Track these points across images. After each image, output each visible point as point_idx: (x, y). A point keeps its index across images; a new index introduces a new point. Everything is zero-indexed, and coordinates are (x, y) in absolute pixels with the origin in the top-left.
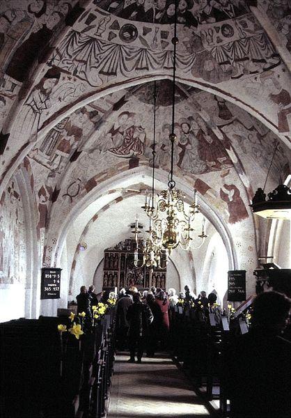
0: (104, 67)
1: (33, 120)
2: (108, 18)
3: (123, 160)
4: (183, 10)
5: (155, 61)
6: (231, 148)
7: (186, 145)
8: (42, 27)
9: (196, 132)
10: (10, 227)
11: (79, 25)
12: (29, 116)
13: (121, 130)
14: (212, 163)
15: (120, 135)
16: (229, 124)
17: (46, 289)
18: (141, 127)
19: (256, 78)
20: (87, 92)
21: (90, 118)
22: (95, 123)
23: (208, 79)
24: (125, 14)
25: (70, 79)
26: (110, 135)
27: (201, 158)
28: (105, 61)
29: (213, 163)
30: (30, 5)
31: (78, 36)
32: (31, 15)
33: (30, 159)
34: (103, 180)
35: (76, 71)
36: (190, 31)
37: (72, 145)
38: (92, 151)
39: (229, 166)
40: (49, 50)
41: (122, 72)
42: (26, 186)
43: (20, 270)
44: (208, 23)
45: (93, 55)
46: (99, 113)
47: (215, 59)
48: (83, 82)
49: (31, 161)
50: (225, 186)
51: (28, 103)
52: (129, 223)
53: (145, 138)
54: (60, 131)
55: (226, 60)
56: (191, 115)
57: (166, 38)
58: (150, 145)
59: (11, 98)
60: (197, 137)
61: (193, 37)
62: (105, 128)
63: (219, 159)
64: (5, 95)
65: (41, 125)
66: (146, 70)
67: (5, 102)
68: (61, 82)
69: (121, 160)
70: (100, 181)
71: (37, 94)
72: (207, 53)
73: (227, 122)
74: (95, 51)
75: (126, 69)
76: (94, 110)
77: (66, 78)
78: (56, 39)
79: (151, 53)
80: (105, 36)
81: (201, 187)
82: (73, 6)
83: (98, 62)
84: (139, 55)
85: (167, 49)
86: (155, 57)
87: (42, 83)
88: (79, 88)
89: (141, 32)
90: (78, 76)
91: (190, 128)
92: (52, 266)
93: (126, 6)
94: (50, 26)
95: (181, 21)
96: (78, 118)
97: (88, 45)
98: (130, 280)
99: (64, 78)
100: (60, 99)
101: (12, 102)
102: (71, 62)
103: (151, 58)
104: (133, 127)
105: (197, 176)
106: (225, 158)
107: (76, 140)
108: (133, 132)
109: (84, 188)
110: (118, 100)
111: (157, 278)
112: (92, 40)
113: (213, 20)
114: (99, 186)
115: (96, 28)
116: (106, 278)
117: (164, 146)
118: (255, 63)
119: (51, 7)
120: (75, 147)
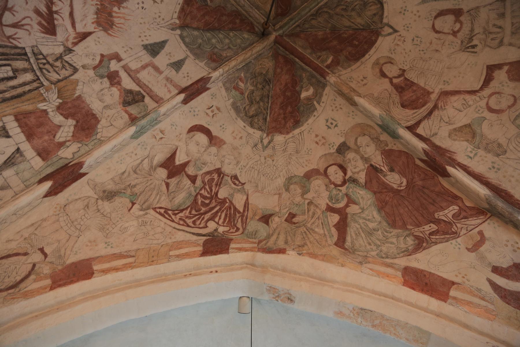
7: (347, 206)
9: (362, 177)
13: (191, 170)
14: (427, 227)
15: (187, 182)
16: (430, 113)
18: (235, 177)
21: (126, 103)
22: (133, 120)
26: (163, 173)
27: (393, 225)
37: (61, 145)
39: (473, 222)
46: (147, 99)
50: (496, 270)
53: (246, 205)
54: (46, 83)
56: (342, 140)
58: (257, 218)
60: (367, 186)
63: (440, 215)
70: (105, 272)
73: (423, 111)
91: (345, 173)
104: (219, 171)
106: (454, 209)
107: (76, 137)
108: (219, 185)
109: (46, 277)
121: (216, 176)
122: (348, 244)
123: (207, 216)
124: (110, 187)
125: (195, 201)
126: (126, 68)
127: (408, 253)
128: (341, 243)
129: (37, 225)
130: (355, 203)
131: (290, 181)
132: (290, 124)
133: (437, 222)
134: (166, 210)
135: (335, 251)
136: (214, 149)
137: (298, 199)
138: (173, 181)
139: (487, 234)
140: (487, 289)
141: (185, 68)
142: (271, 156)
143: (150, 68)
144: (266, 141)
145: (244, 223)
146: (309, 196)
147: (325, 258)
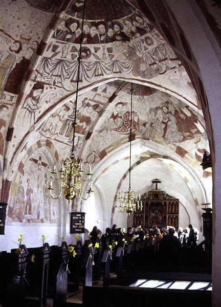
0: (73, 78)
1: (30, 117)
2: (67, 45)
3: (124, 136)
4: (118, 32)
5: (107, 69)
6: (198, 122)
7: (168, 122)
8: (22, 59)
9: (173, 112)
10: (38, 186)
11: (47, 53)
12: (27, 115)
13: (119, 115)
14: (187, 133)
15: (119, 119)
17: (74, 227)
19: (175, 72)
20: (64, 95)
21: (95, 109)
22: (99, 112)
23: (144, 76)
24: (79, 40)
25: (51, 88)
26: (112, 119)
27: (179, 131)
28: (73, 73)
29: (188, 134)
30: (10, 47)
31: (49, 60)
32: (13, 53)
33: (52, 141)
34: (111, 151)
35: (54, 83)
36: (126, 45)
37: (85, 129)
38: (101, 131)
40: (30, 72)
41: (85, 79)
42: (52, 159)
43: (52, 214)
44: (136, 37)
45: (64, 71)
46: (100, 105)
47: (146, 62)
48: (61, 89)
49: (53, 142)
50: (199, 150)
51: (25, 106)
52: (151, 180)
53: (138, 120)
55: (153, 62)
57: (112, 52)
59: (12, 105)
60: (175, 115)
61: (129, 49)
62: (106, 115)
64: (7, 104)
65: (36, 119)
66: (102, 76)
67: (7, 108)
68: (45, 91)
69: (122, 136)
71: (30, 100)
72: (140, 59)
74: (64, 68)
75: (88, 77)
76: (96, 103)
77: (49, 88)
78: (34, 65)
79: (104, 64)
80: (69, 58)
81: (181, 152)
82: (39, 42)
83: (69, 75)
84: (81, 67)
85: (113, 59)
86: (107, 66)
87: (31, 93)
88: (59, 93)
89: (93, 51)
90: (57, 86)
92: (79, 211)
93: (77, 36)
94: (27, 57)
95: (119, 39)
96: (85, 110)
97: (58, 66)
98: (153, 221)
99: (47, 88)
100: (47, 102)
101: (13, 107)
102: (50, 77)
103: (104, 67)
104: (128, 112)
105: (177, 144)
106: (196, 130)
107: (87, 125)
110: (111, 95)
111: (172, 219)
112: (60, 61)
113: (138, 35)
114: (108, 155)
115: (61, 53)
116: (135, 219)
117: (152, 124)
118: (173, 61)
119: (25, 45)
120: (87, 130)
121: (127, 114)
122: (166, 136)
123: (128, 127)
124: (101, 129)
125: (123, 123)
126: (90, 100)
127: (180, 141)
128: (164, 136)
129: (90, 146)
130: (171, 121)
131: (151, 110)
132: (149, 93)
133: (191, 132)
134: (116, 129)
135: (162, 139)
136: (125, 107)
137: (154, 117)
138: (115, 120)
139: (201, 139)
140: (194, 154)
141: (108, 91)
142: (144, 102)
143: (97, 96)
144: (141, 98)
145: (139, 127)
146: (157, 116)
147: (159, 142)
